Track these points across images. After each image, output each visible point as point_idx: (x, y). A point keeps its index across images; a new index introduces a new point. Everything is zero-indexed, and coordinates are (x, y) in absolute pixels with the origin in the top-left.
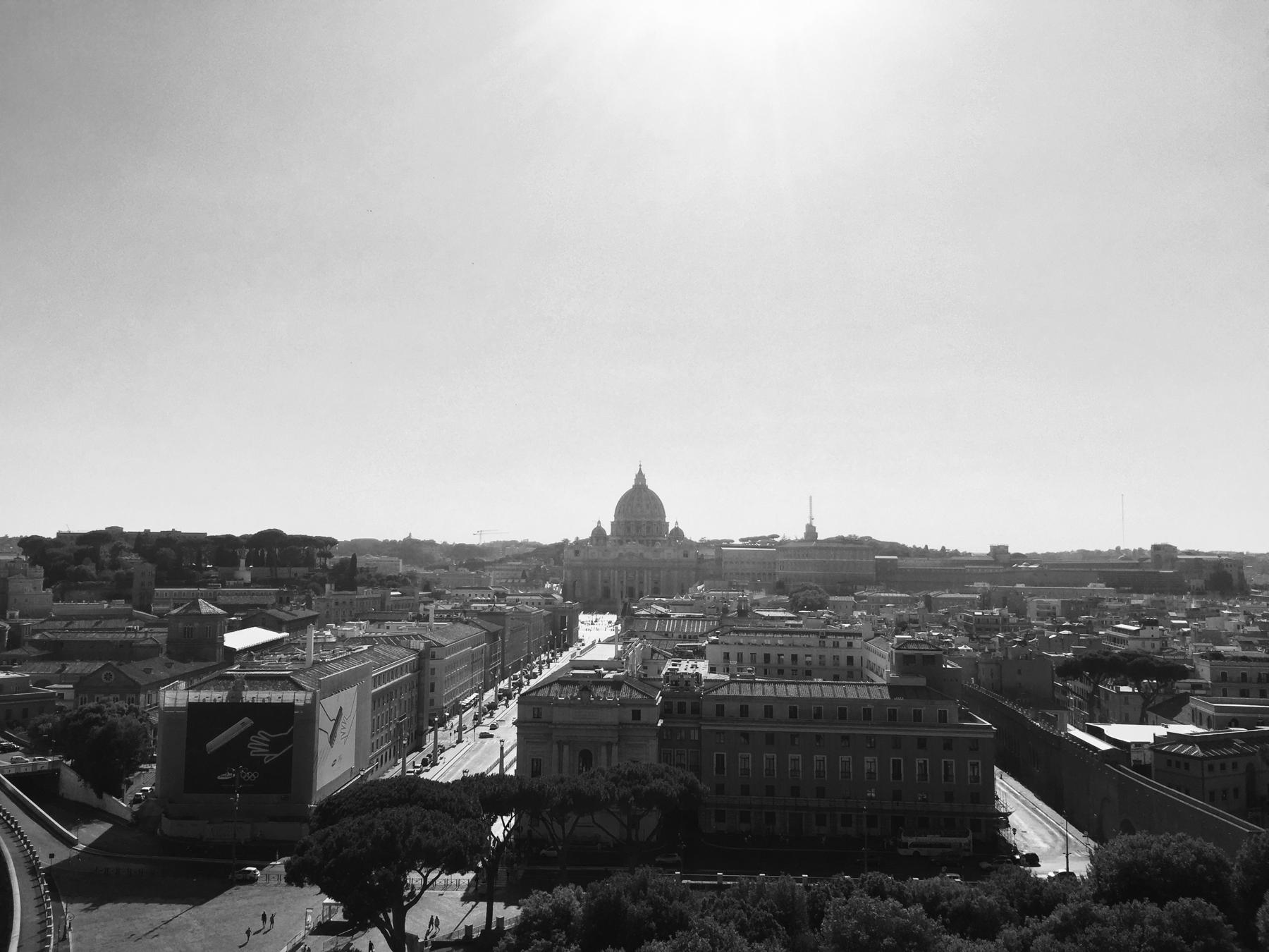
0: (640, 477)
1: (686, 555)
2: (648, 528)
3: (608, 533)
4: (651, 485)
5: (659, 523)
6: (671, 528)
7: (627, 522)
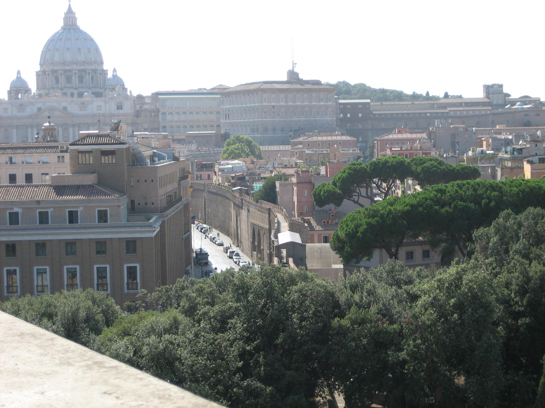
0: (70, 18)
1: (120, 107)
2: (81, 79)
3: (33, 86)
4: (83, 24)
5: (95, 71)
6: (110, 75)
7: (54, 71)
